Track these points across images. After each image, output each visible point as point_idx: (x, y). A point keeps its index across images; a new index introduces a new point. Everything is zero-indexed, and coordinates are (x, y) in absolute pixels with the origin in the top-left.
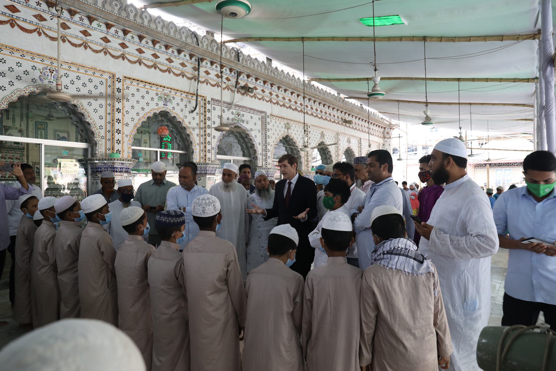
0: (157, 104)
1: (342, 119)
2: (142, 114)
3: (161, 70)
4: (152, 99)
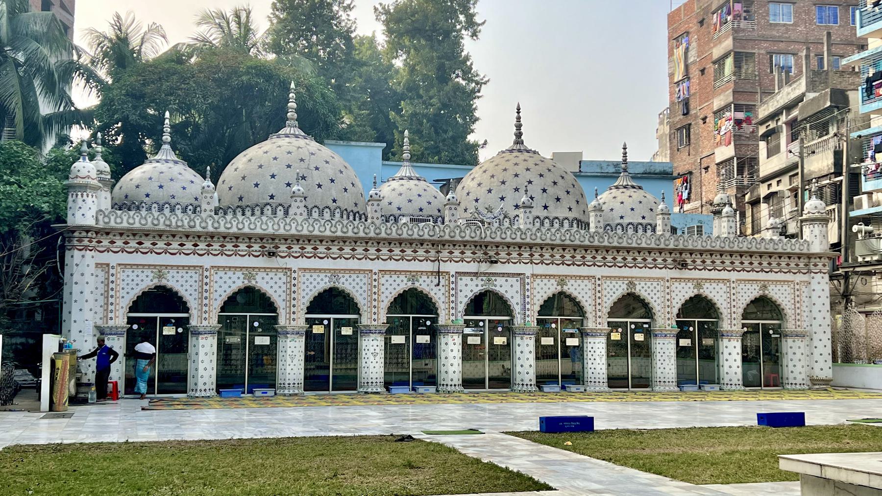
1: (674, 261)
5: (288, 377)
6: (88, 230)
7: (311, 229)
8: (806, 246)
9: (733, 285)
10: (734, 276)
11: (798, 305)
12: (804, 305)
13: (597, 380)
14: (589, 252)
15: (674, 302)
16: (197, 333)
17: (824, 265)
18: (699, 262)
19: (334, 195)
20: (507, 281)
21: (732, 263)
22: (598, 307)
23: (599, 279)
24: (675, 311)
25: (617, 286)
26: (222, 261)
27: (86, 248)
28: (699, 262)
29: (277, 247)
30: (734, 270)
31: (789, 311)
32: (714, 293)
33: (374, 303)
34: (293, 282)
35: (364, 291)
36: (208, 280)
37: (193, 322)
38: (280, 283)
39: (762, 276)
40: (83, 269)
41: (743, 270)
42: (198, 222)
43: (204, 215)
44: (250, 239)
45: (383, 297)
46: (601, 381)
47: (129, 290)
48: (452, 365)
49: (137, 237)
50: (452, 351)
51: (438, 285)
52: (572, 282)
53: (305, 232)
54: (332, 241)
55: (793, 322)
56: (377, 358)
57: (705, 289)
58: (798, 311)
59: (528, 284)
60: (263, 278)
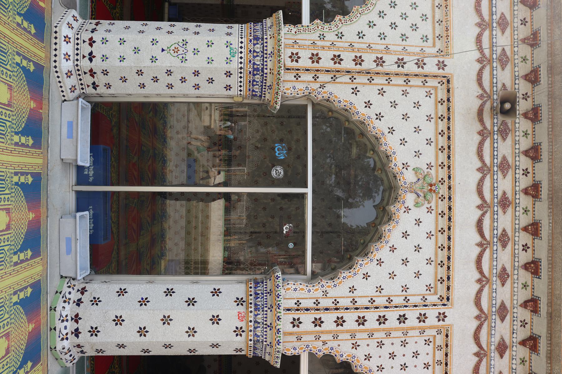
10: (462, 318)
15: (368, 92)
18: (505, 184)
21: (503, 311)
28: (505, 184)
30: (482, 317)
32: (405, 248)
57: (416, 213)
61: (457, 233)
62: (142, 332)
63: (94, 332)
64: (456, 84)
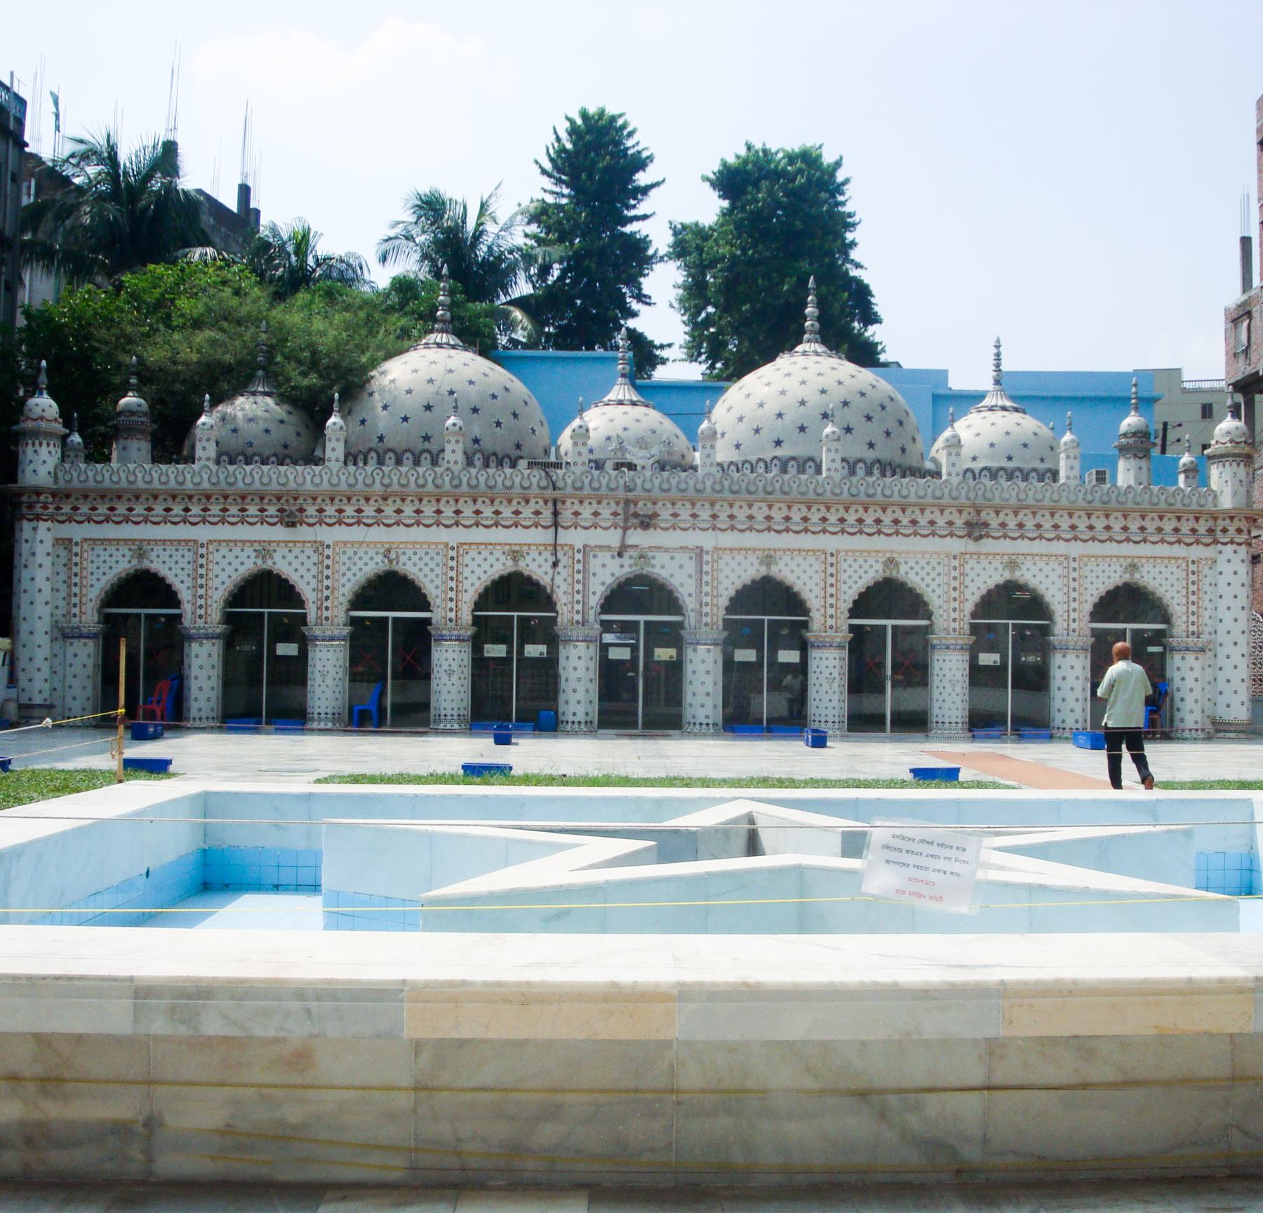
0: (504, 564)
2: (484, 577)
3: (504, 526)
4: (498, 559)
5: (317, 703)
6: (38, 492)
7: (352, 481)
8: (1210, 498)
9: (1075, 565)
10: (1076, 549)
11: (1192, 598)
12: (1207, 598)
13: (823, 720)
14: (814, 509)
15: (968, 593)
16: (191, 638)
17: (1239, 531)
19: (477, 431)
20: (672, 558)
22: (831, 601)
23: (832, 555)
24: (969, 607)
25: (866, 566)
26: (223, 532)
27: (38, 518)
29: (302, 510)
31: (1177, 608)
32: (1041, 577)
33: (452, 594)
34: (327, 562)
35: (437, 576)
36: (203, 561)
37: (187, 622)
38: (309, 564)
39: (1128, 549)
40: (39, 544)
41: (1093, 539)
42: (188, 477)
43: (196, 466)
44: (262, 499)
45: (467, 585)
46: (831, 719)
47: (100, 576)
48: (574, 691)
49: (106, 500)
50: (575, 669)
51: (555, 565)
52: (786, 559)
53: (343, 486)
54: (385, 499)
55: (1184, 627)
56: (454, 678)
58: (1193, 608)
59: (707, 563)
60: (284, 557)
61: (1035, 551)
62: (1077, 700)
63: (1077, 722)
64: (963, 550)
